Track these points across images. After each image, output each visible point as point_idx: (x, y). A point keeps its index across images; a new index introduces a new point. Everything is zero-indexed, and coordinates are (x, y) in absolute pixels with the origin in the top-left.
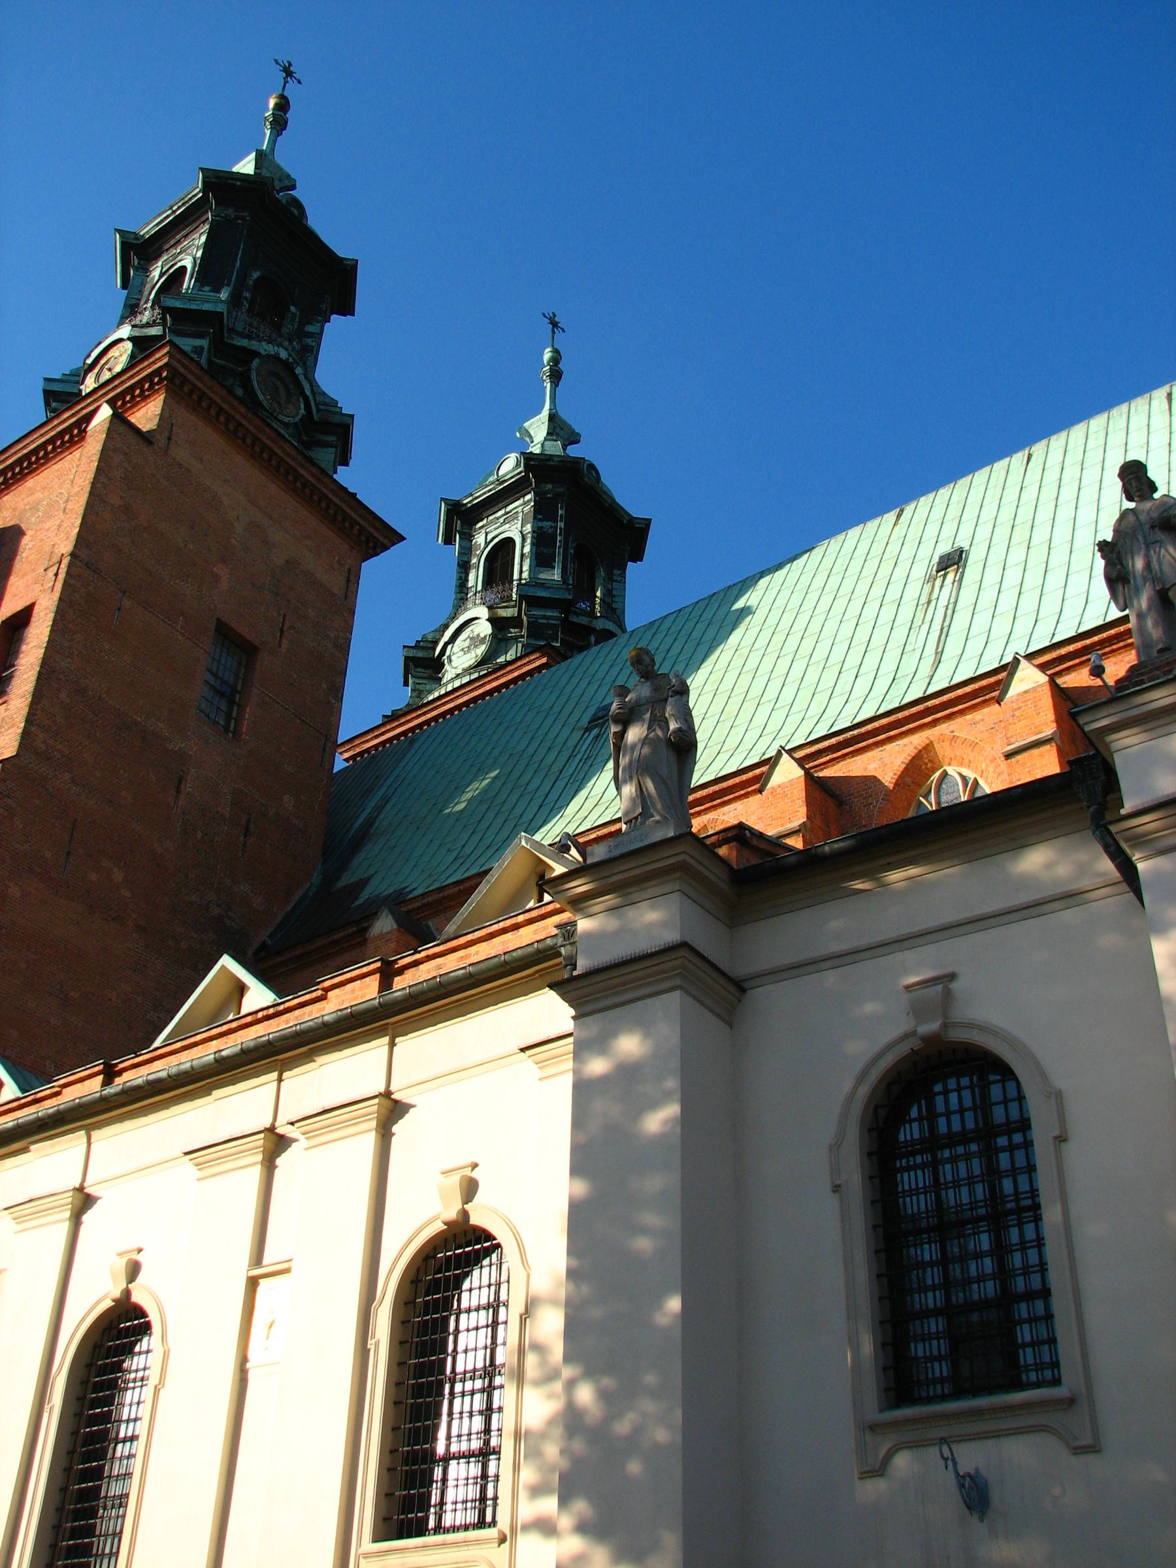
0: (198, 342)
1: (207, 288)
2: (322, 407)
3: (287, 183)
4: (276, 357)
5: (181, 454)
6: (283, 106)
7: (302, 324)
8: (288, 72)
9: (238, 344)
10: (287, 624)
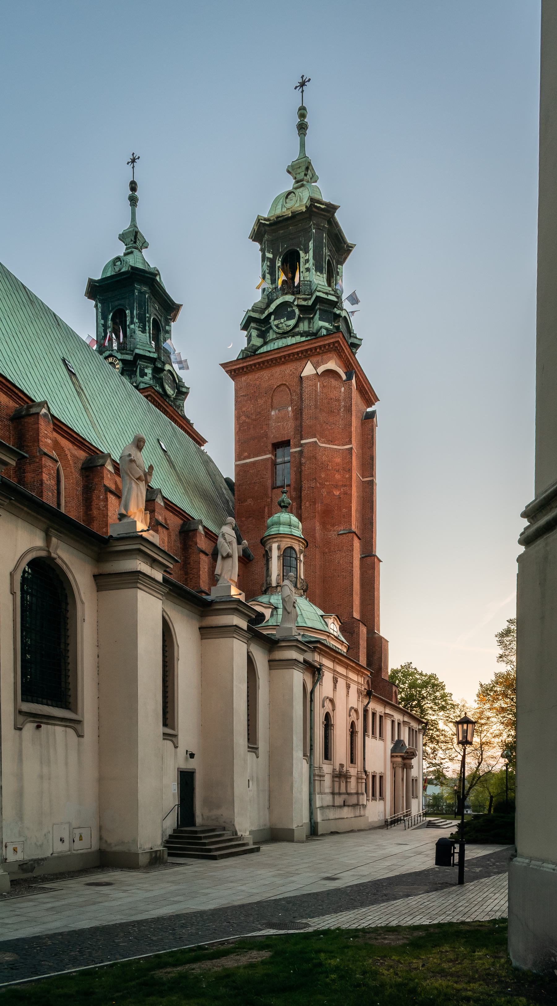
6: (133, 186)
7: (132, 313)
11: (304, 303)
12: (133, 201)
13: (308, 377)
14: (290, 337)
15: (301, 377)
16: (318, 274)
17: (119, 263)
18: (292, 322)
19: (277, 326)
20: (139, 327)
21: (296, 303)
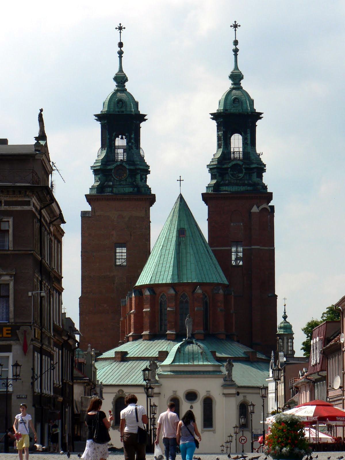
0: (99, 176)
1: (104, 149)
2: (136, 163)
3: (125, 79)
4: (118, 166)
5: (98, 214)
6: (121, 45)
8: (120, 28)
9: (108, 168)
10: (132, 233)
11: (248, 166)
12: (121, 53)
13: (255, 213)
14: (242, 187)
15: (251, 213)
16: (252, 147)
17: (121, 103)
18: (241, 175)
19: (232, 175)
20: (135, 146)
21: (244, 166)
